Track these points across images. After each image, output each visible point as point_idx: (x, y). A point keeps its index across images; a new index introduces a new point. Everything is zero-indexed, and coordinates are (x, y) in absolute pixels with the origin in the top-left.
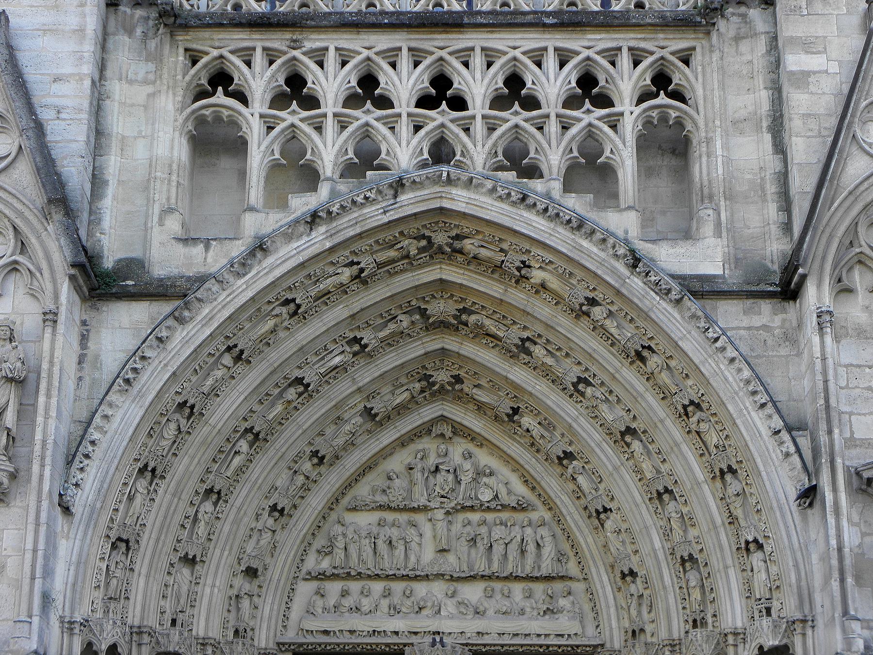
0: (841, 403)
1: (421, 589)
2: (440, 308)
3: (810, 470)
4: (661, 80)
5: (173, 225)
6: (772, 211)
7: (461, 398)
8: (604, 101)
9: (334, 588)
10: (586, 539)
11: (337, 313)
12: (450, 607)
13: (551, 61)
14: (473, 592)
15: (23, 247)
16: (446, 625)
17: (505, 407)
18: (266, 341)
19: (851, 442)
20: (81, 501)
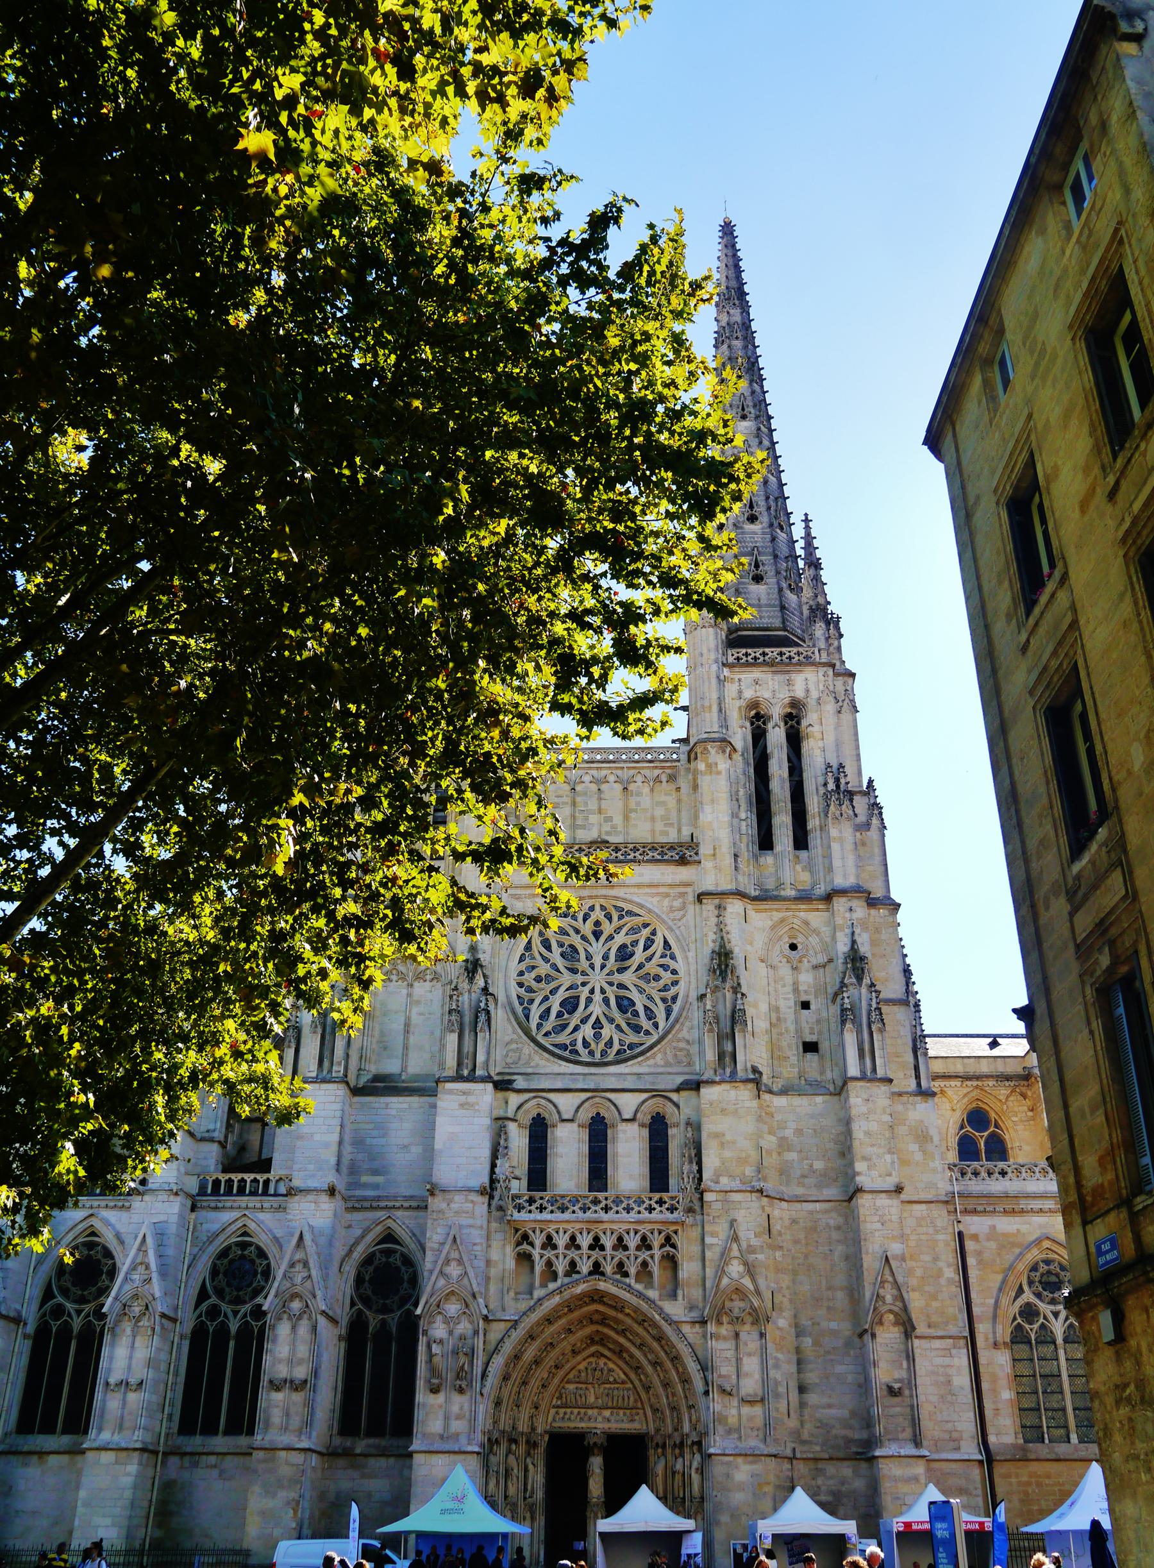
0: (717, 1362)
1: (590, 1412)
2: (596, 1317)
3: (707, 1384)
4: (668, 1239)
5: (512, 1294)
6: (700, 1291)
7: (604, 1345)
8: (649, 1248)
9: (562, 1411)
10: (644, 1396)
11: (563, 1321)
12: (600, 1419)
13: (632, 1233)
14: (607, 1413)
15: (467, 1306)
16: (599, 1426)
17: (617, 1349)
18: (542, 1332)
19: (720, 1376)
20: (485, 1391)
